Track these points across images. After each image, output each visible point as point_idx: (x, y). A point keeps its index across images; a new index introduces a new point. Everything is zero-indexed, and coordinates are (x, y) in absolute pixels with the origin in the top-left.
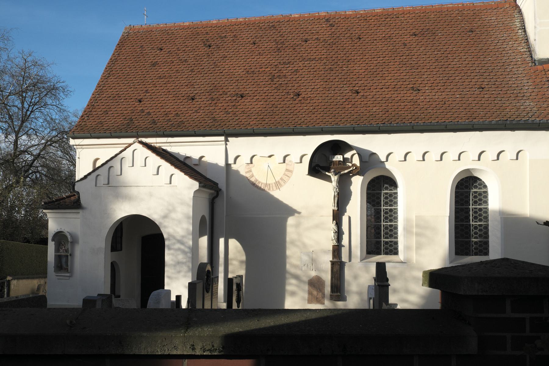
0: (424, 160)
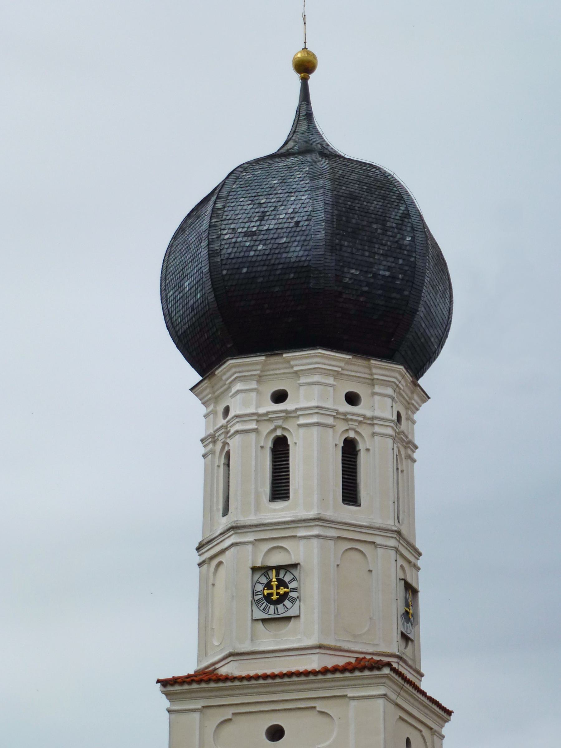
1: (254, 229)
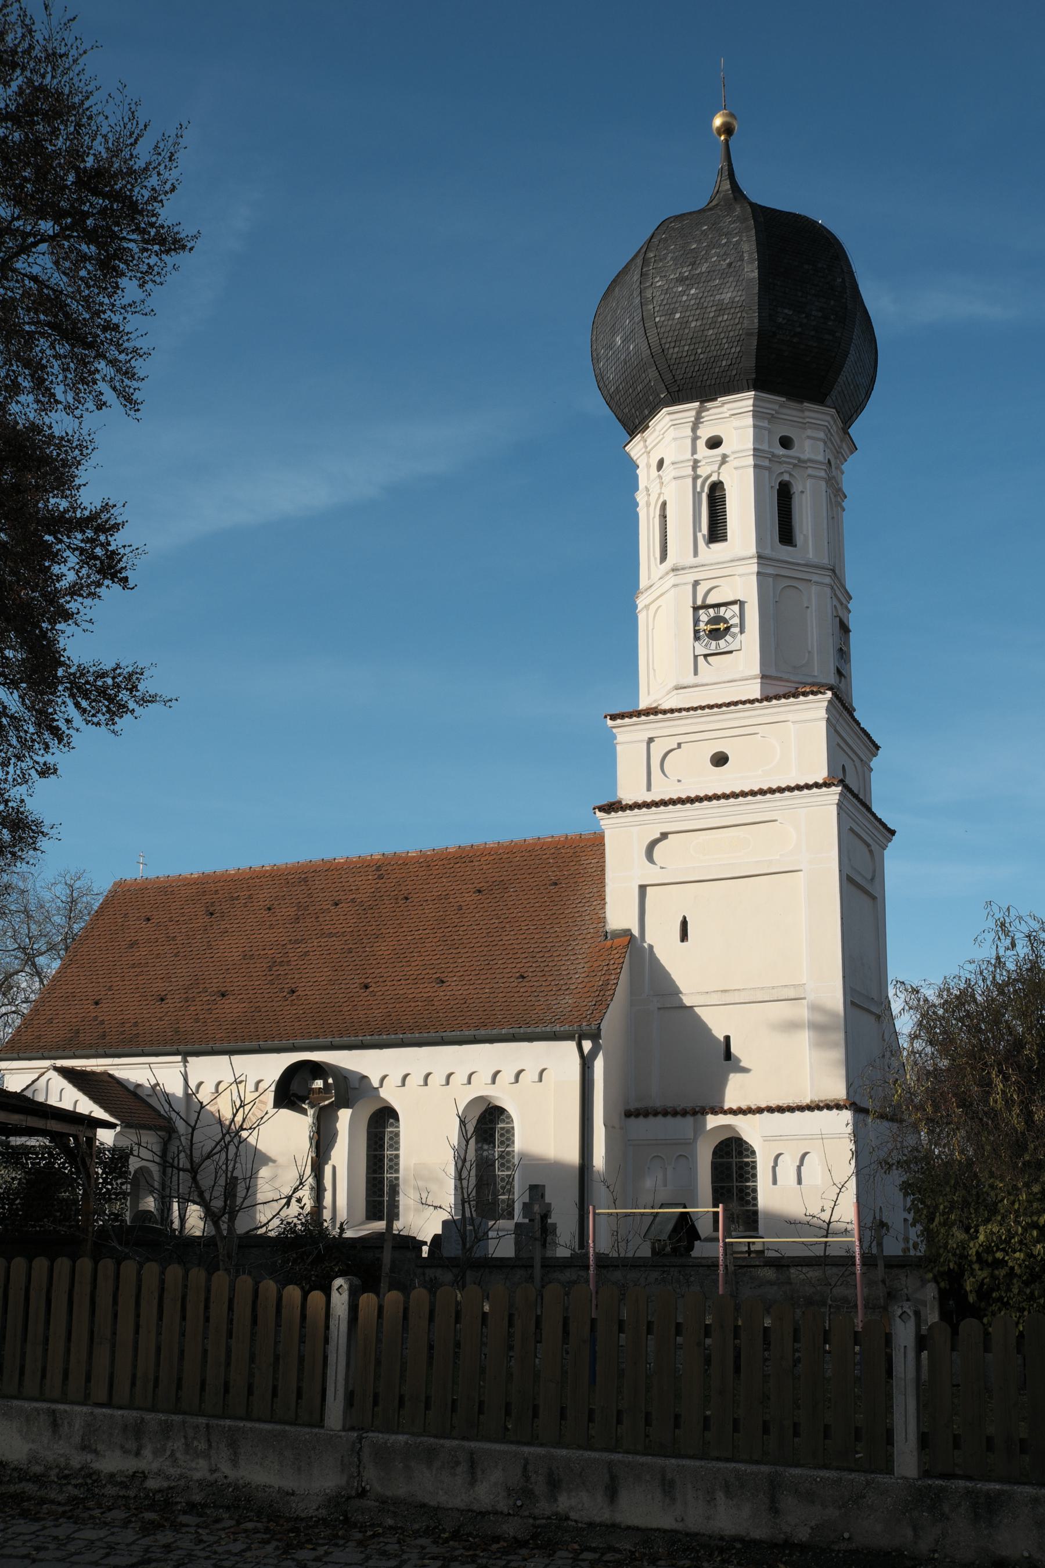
0: (426, 1084)
1: (686, 274)
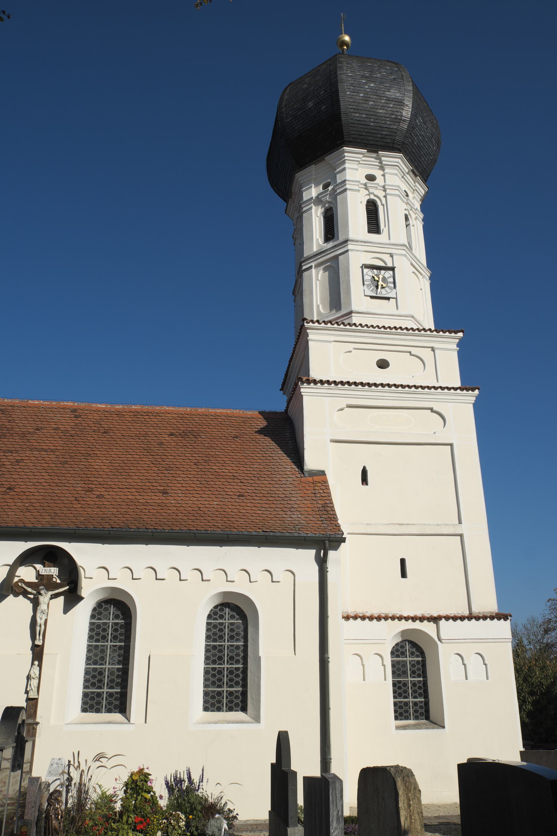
1: (368, 75)
